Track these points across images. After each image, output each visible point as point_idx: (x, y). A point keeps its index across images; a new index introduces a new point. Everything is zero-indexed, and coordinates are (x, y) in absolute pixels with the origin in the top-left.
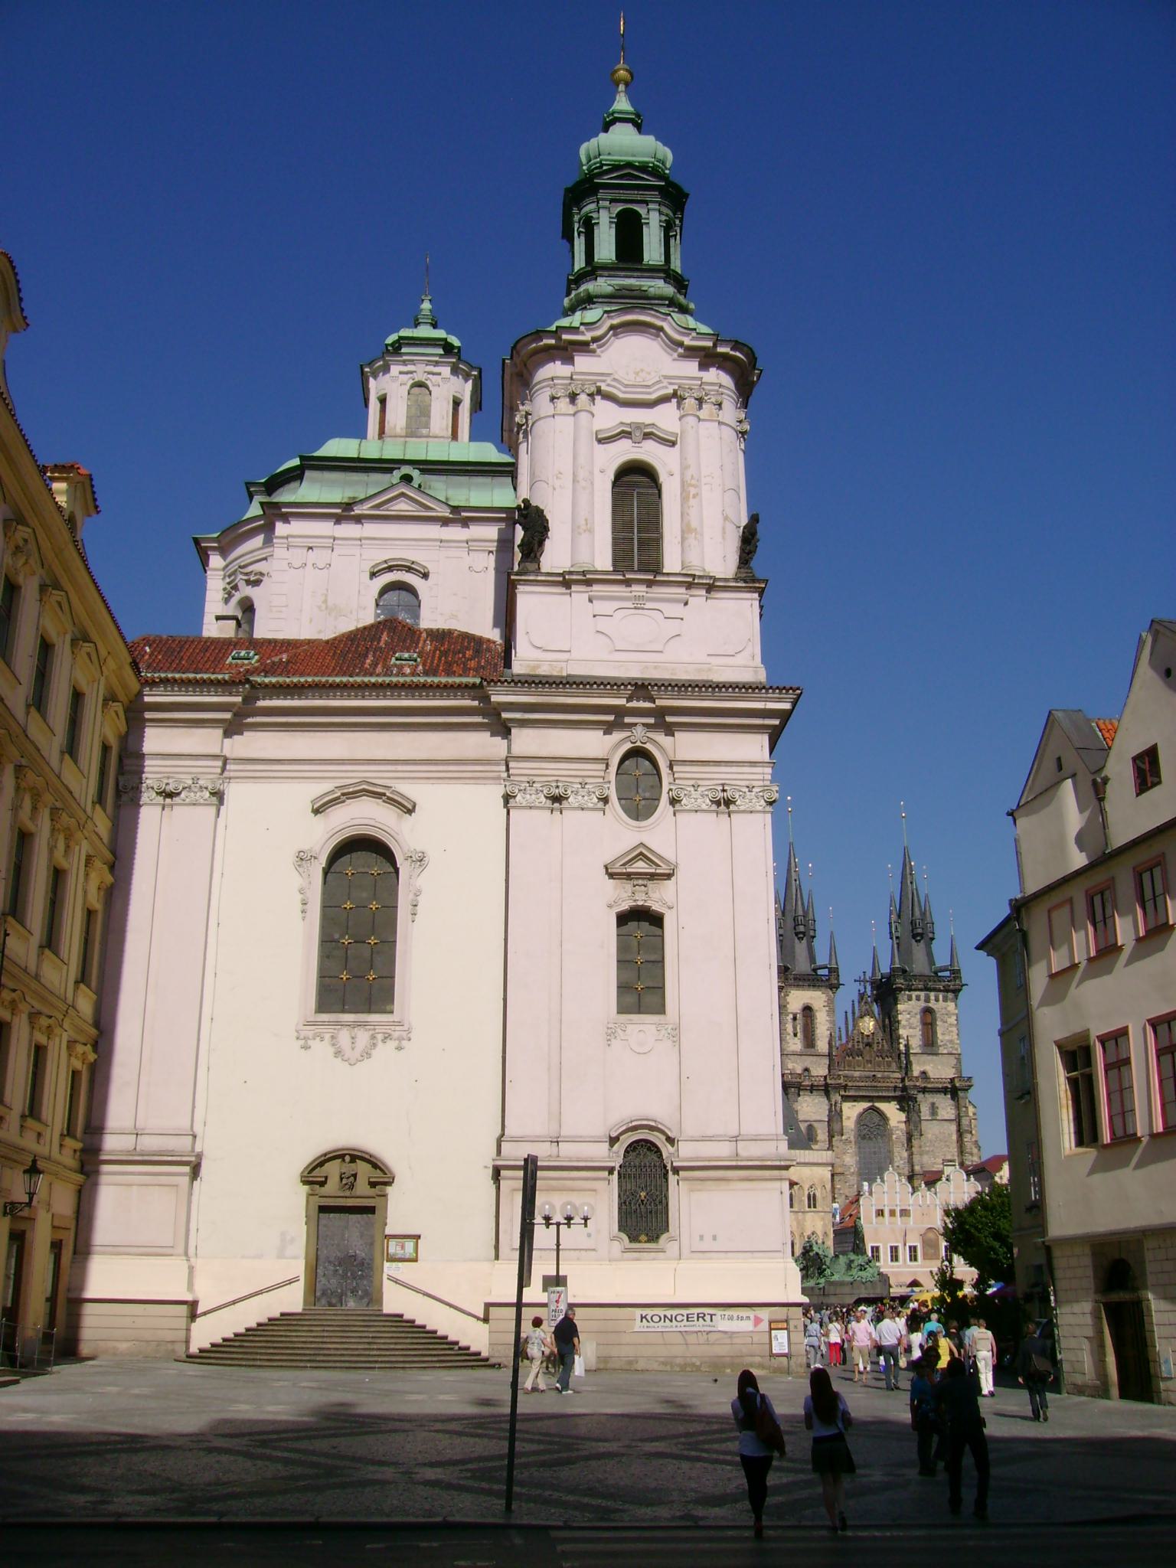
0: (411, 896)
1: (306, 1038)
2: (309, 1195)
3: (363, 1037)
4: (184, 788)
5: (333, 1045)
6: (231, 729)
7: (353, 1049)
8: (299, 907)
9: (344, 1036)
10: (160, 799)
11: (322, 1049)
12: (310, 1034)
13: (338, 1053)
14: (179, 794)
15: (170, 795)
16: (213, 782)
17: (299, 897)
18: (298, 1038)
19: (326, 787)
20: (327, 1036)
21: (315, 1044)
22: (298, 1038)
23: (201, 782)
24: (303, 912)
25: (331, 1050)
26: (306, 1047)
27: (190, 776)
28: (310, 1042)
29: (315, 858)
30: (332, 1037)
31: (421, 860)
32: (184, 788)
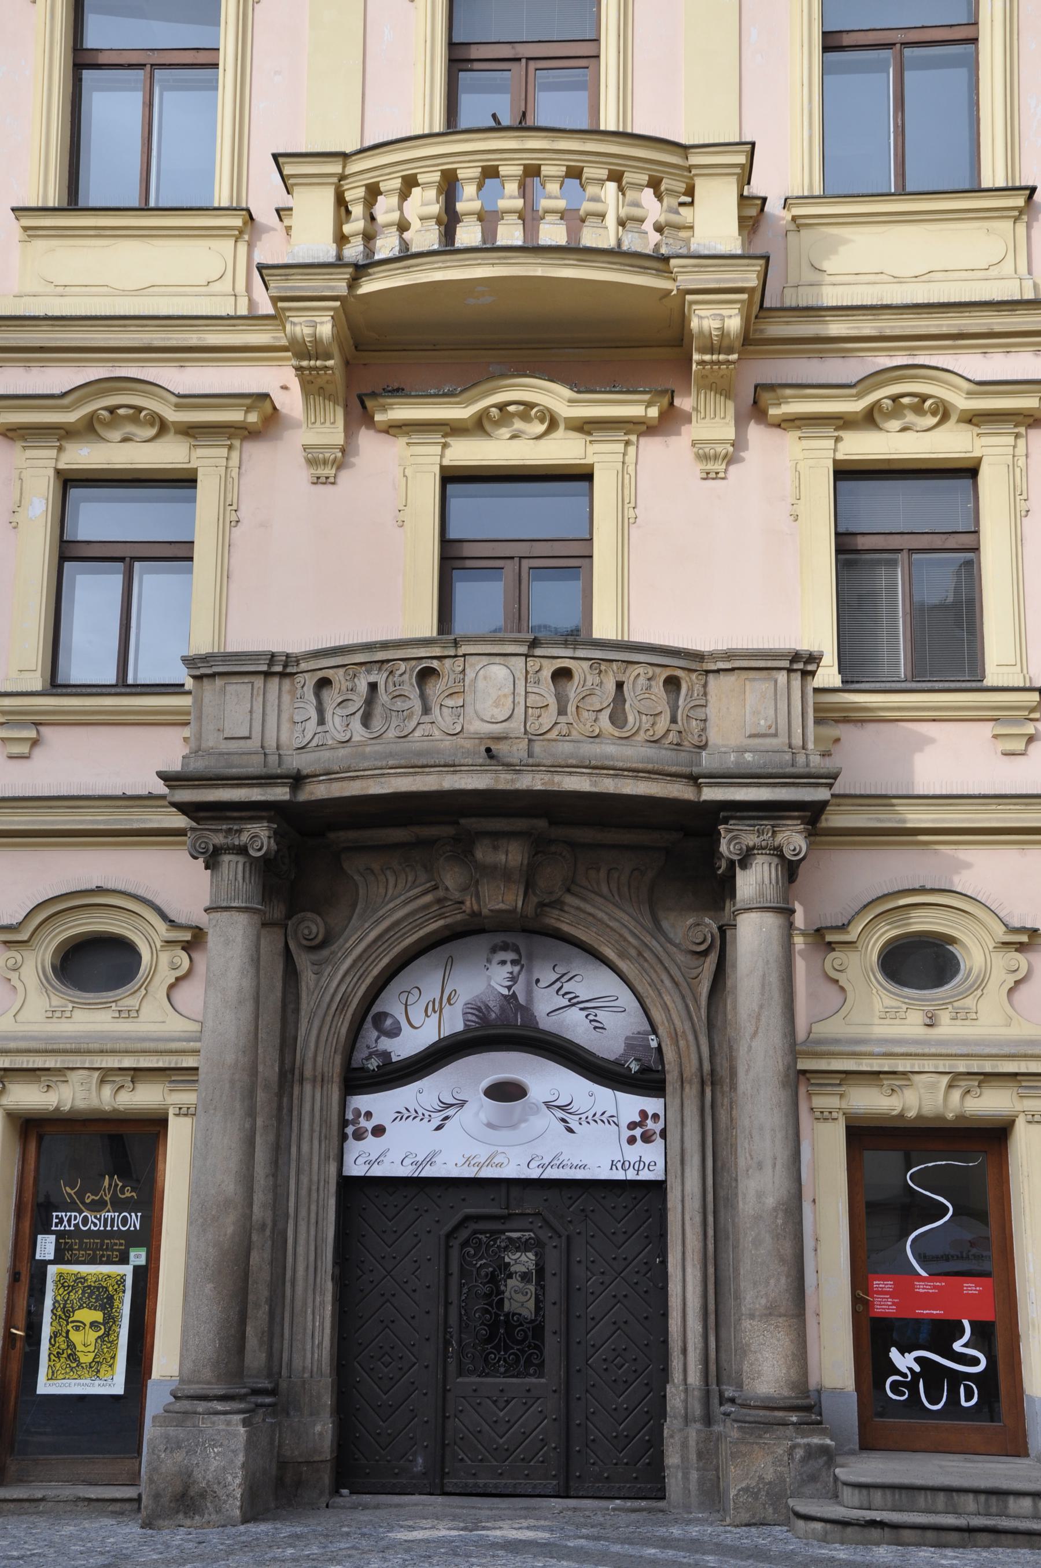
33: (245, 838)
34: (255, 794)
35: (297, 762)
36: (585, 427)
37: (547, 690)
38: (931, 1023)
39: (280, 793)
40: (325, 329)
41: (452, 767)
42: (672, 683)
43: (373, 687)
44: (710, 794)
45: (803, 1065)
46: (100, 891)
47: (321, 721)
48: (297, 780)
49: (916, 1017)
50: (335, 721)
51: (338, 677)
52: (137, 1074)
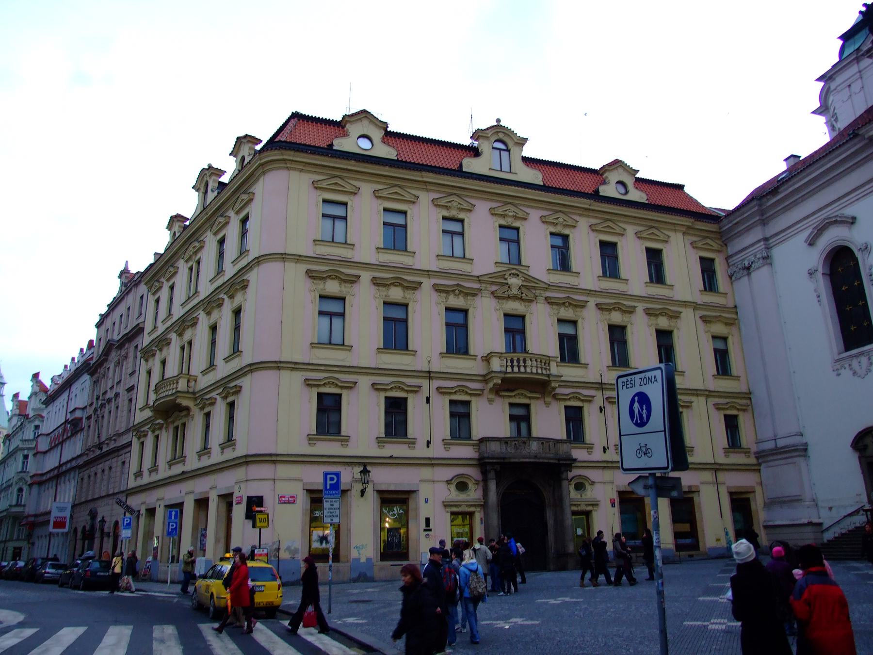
0: (868, 271)
1: (837, 370)
2: (860, 458)
3: (864, 360)
4: (752, 263)
5: (851, 369)
6: (764, 223)
7: (861, 368)
8: (816, 300)
9: (855, 363)
10: (745, 272)
11: (846, 373)
12: (839, 367)
13: (855, 373)
14: (751, 266)
15: (748, 268)
16: (761, 253)
17: (815, 294)
18: (833, 371)
19: (805, 234)
20: (847, 366)
21: (842, 371)
22: (833, 371)
23: (758, 256)
24: (819, 301)
25: (851, 373)
26: (839, 375)
27: (752, 256)
28: (840, 371)
29: (817, 270)
30: (850, 365)
31: (866, 248)
32: (752, 263)
33: (495, 467)
34: (499, 461)
35: (502, 456)
36: (530, 398)
37: (541, 446)
38: (581, 496)
39: (502, 461)
40: (500, 382)
41: (530, 458)
42: (555, 444)
43: (515, 444)
44: (561, 462)
45: (571, 503)
46: (463, 474)
47: (507, 449)
48: (504, 458)
49: (579, 495)
50: (509, 449)
51: (509, 442)
52: (472, 506)
